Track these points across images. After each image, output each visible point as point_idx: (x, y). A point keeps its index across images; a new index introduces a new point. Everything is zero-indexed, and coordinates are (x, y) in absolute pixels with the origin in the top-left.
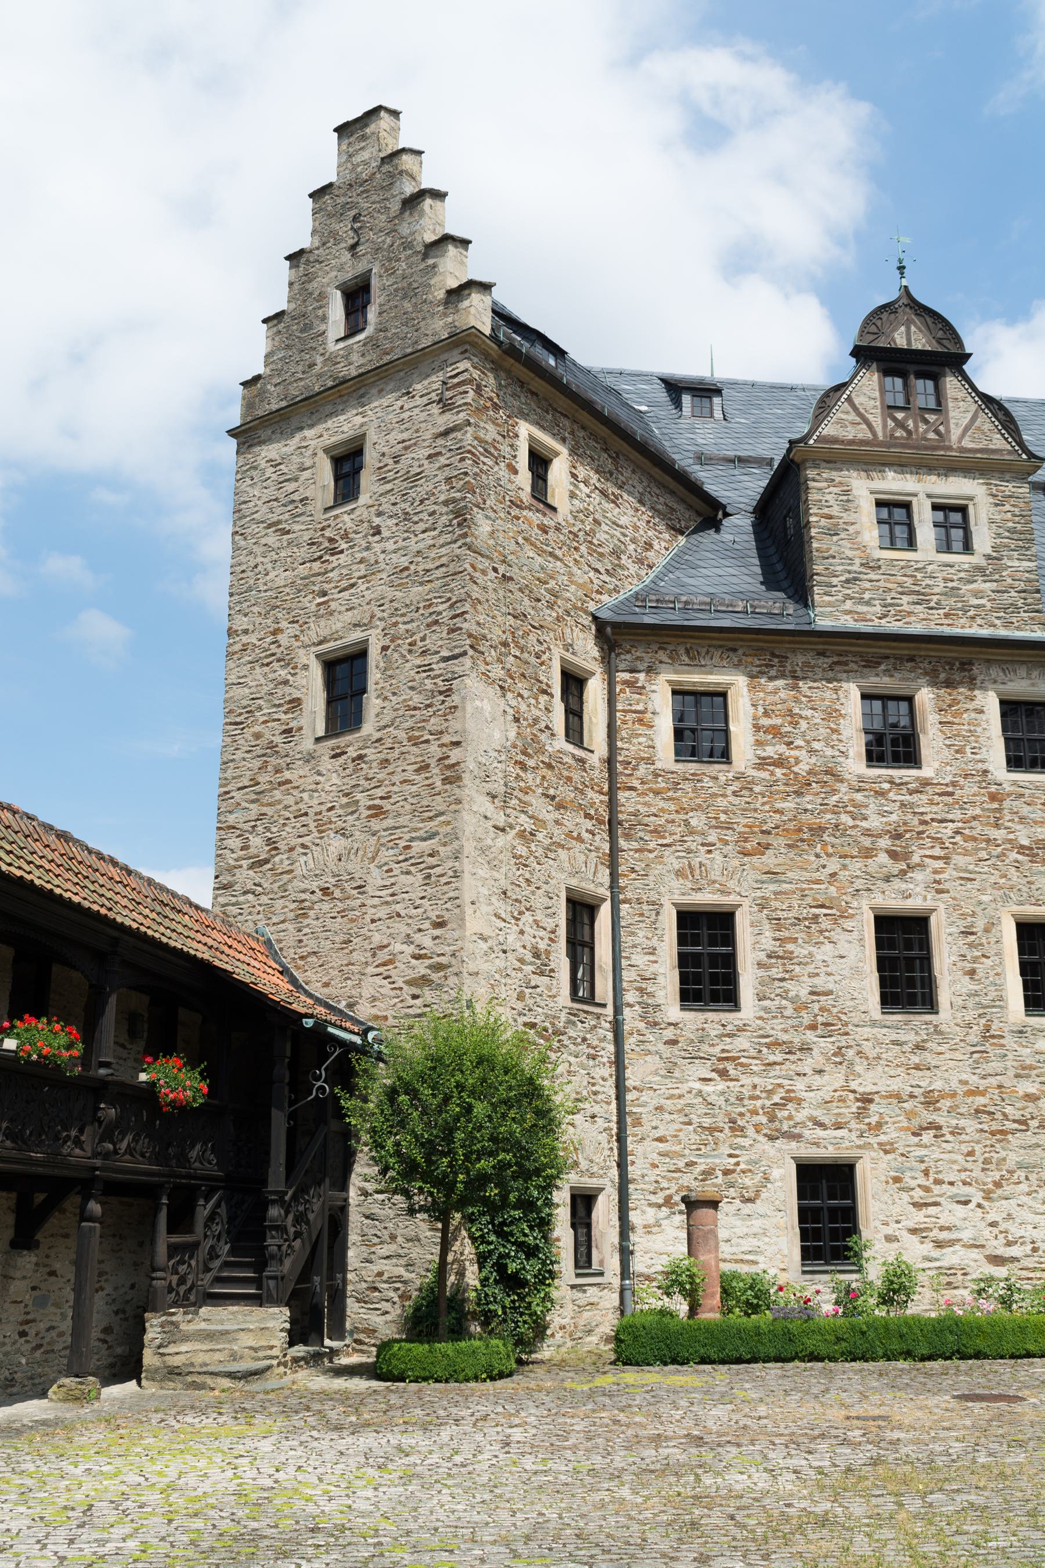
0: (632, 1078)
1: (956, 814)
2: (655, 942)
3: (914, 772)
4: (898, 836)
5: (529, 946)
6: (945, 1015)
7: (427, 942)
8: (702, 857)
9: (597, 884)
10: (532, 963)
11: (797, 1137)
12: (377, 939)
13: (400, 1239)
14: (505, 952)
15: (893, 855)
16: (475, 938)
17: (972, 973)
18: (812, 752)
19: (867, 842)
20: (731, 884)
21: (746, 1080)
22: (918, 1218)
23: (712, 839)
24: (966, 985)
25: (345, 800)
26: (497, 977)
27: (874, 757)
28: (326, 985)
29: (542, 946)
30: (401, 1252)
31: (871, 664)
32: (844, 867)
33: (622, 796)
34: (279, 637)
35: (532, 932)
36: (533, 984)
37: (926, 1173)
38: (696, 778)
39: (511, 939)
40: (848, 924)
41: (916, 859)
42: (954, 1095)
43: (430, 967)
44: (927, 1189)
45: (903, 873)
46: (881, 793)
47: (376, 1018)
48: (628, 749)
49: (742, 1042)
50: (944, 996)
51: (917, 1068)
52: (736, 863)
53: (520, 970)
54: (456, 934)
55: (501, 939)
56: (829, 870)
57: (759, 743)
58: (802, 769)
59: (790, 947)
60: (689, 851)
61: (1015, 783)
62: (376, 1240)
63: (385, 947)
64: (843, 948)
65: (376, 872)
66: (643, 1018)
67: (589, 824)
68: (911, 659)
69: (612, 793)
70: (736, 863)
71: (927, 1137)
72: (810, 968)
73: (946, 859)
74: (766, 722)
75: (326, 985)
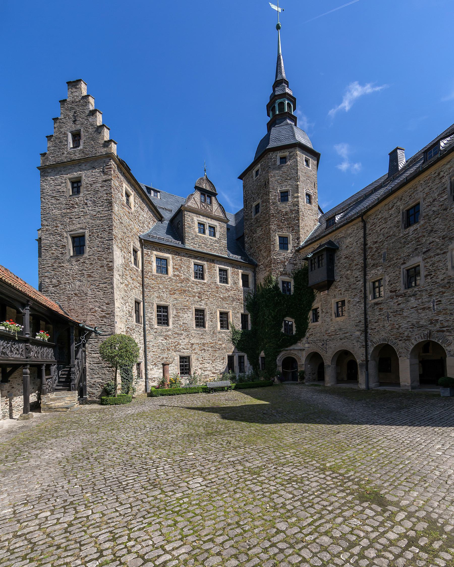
0: (148, 339)
1: (210, 290)
2: (152, 311)
3: (203, 281)
4: (200, 294)
6: (207, 329)
7: (105, 308)
8: (162, 294)
9: (140, 298)
11: (180, 351)
12: (91, 306)
15: (199, 297)
17: (212, 321)
18: (184, 274)
19: (194, 294)
20: (168, 300)
21: (170, 340)
22: (201, 366)
23: (164, 290)
24: (211, 323)
25: (80, 272)
27: (196, 277)
29: (130, 311)
31: (196, 258)
32: (190, 299)
33: (145, 279)
34: (58, 228)
37: (202, 358)
38: (161, 277)
40: (190, 310)
41: (203, 298)
42: (208, 343)
43: (106, 314)
44: (203, 361)
45: (200, 301)
46: (197, 285)
48: (146, 269)
49: (170, 333)
50: (207, 325)
51: (202, 338)
52: (169, 296)
54: (112, 307)
56: (187, 299)
57: (174, 271)
58: (182, 278)
59: (179, 314)
60: (159, 293)
61: (221, 285)
64: (189, 315)
65: (90, 291)
66: (150, 327)
67: (139, 285)
68: (204, 258)
69: (143, 278)
70: (169, 296)
71: (203, 352)
72: (183, 319)
73: (208, 299)
74: (176, 267)
75: (77, 317)
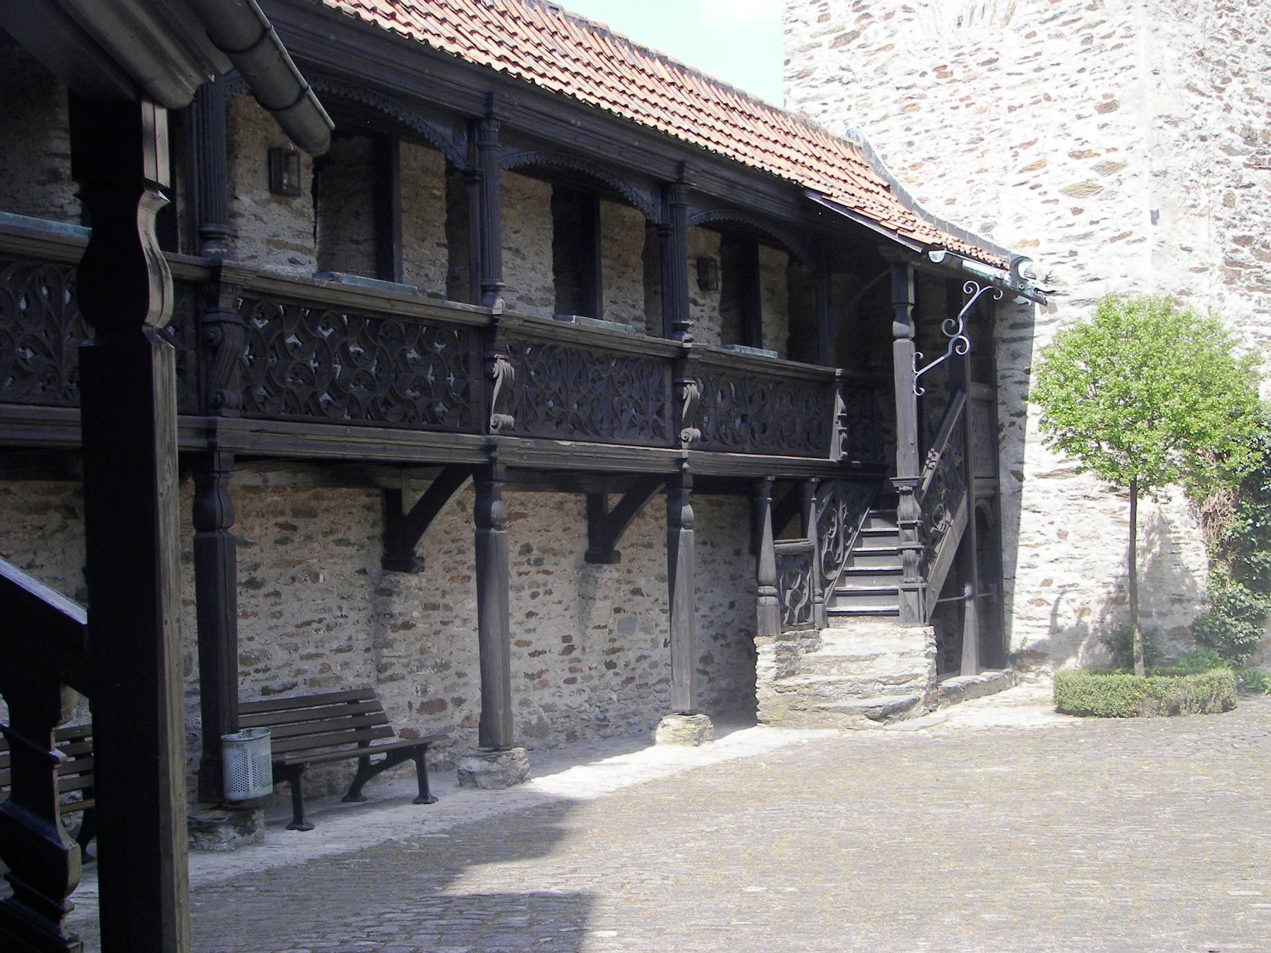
5: (1238, 128)
10: (1242, 153)
12: (1018, 135)
13: (1071, 537)
14: (1203, 139)
16: (1160, 122)
26: (1194, 175)
28: (951, 202)
30: (1076, 552)
35: (1243, 106)
36: (1246, 181)
39: (1212, 118)
47: (1024, 243)
53: (1227, 163)
55: (1198, 120)
62: (1040, 539)
63: (1030, 144)
75: (951, 202)
